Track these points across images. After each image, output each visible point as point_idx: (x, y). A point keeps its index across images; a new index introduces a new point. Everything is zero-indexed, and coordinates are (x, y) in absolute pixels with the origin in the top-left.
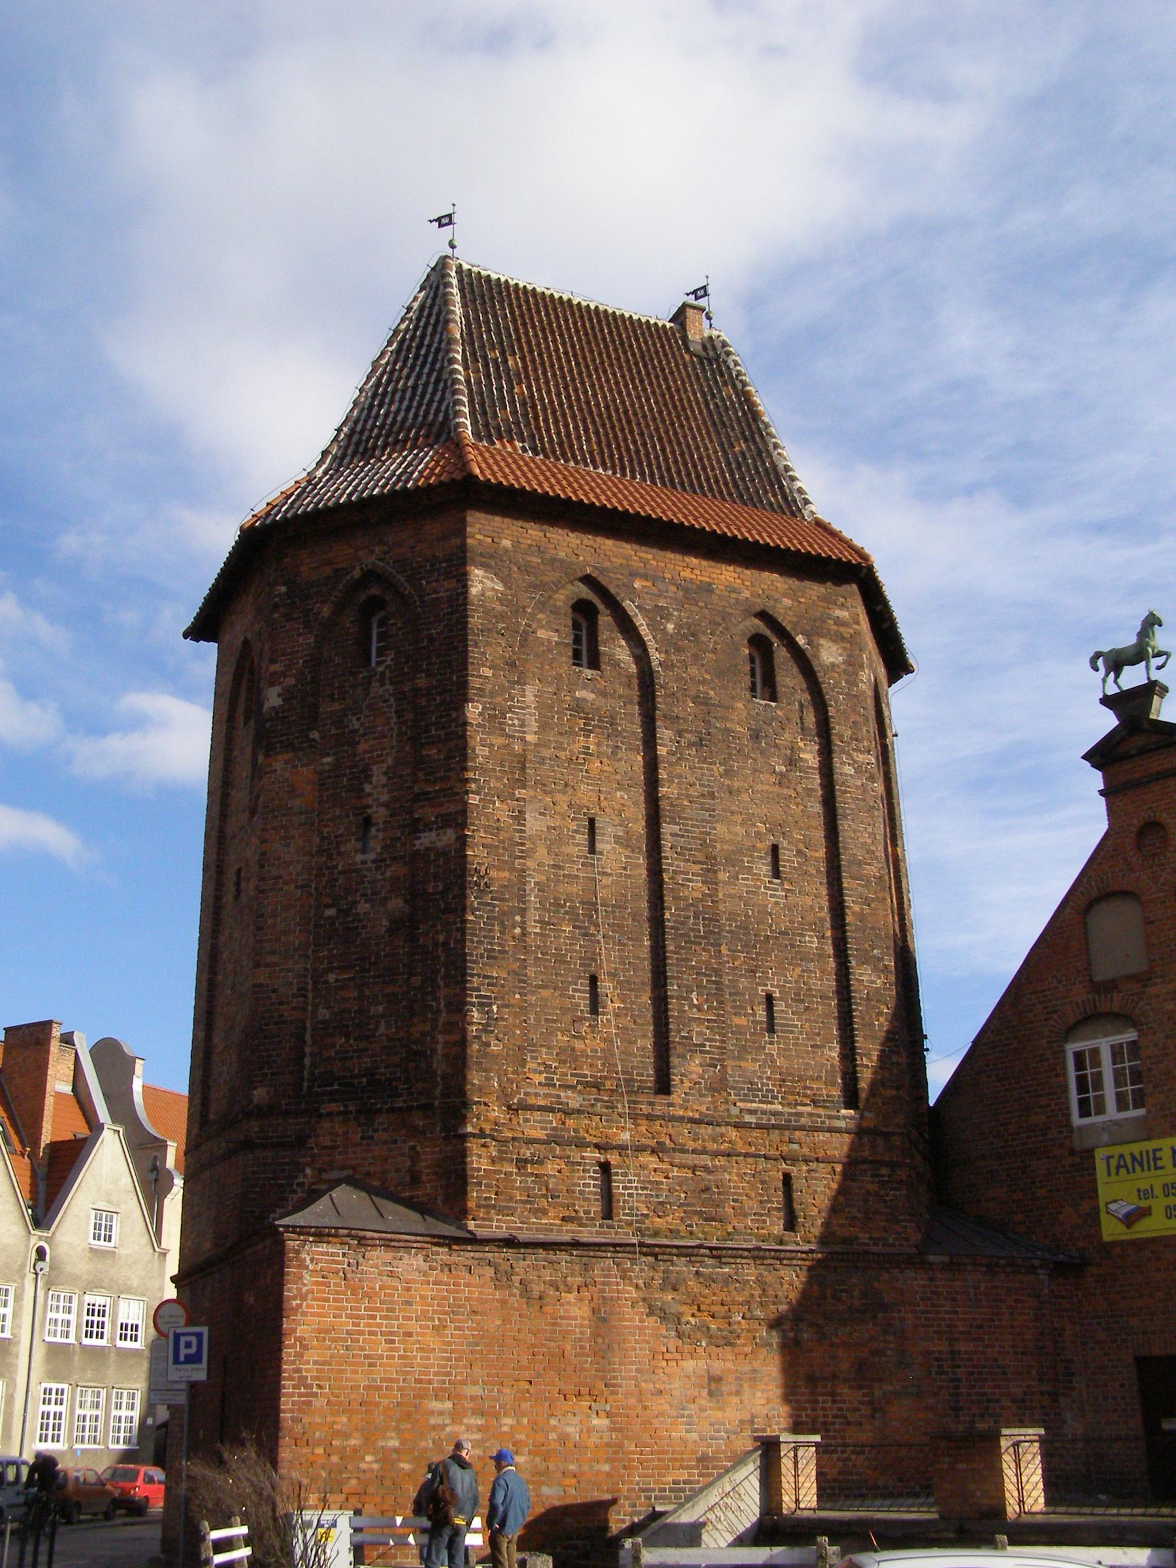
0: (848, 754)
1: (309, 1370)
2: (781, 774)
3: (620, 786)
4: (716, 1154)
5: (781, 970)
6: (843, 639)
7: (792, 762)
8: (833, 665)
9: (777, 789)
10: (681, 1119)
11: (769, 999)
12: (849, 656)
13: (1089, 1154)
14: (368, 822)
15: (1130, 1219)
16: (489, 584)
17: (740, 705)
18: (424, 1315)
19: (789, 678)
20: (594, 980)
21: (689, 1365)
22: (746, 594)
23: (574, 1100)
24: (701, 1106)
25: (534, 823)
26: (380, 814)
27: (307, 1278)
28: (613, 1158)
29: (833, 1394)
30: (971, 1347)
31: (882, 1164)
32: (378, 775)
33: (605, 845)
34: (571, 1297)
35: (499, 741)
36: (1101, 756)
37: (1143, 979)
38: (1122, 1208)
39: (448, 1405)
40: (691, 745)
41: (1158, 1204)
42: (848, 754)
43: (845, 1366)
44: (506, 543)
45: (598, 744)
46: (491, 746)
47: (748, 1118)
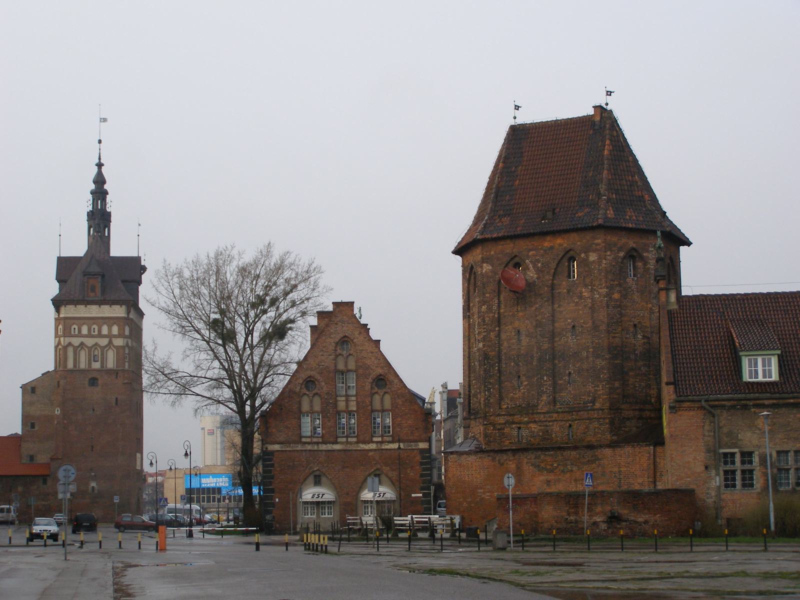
0: (597, 291)
2: (577, 302)
3: (527, 319)
4: (549, 422)
6: (598, 250)
7: (581, 297)
8: (594, 261)
9: (575, 307)
10: (540, 413)
11: (570, 373)
12: (600, 256)
16: (488, 268)
17: (564, 283)
18: (476, 470)
20: (519, 377)
21: (542, 478)
22: (565, 245)
24: (545, 410)
25: (503, 336)
27: (450, 463)
28: (522, 426)
29: (582, 484)
30: (625, 469)
31: (600, 418)
33: (523, 338)
34: (511, 463)
35: (492, 315)
39: (482, 491)
40: (546, 301)
42: (597, 291)
44: (492, 253)
45: (521, 308)
46: (489, 317)
47: (559, 410)
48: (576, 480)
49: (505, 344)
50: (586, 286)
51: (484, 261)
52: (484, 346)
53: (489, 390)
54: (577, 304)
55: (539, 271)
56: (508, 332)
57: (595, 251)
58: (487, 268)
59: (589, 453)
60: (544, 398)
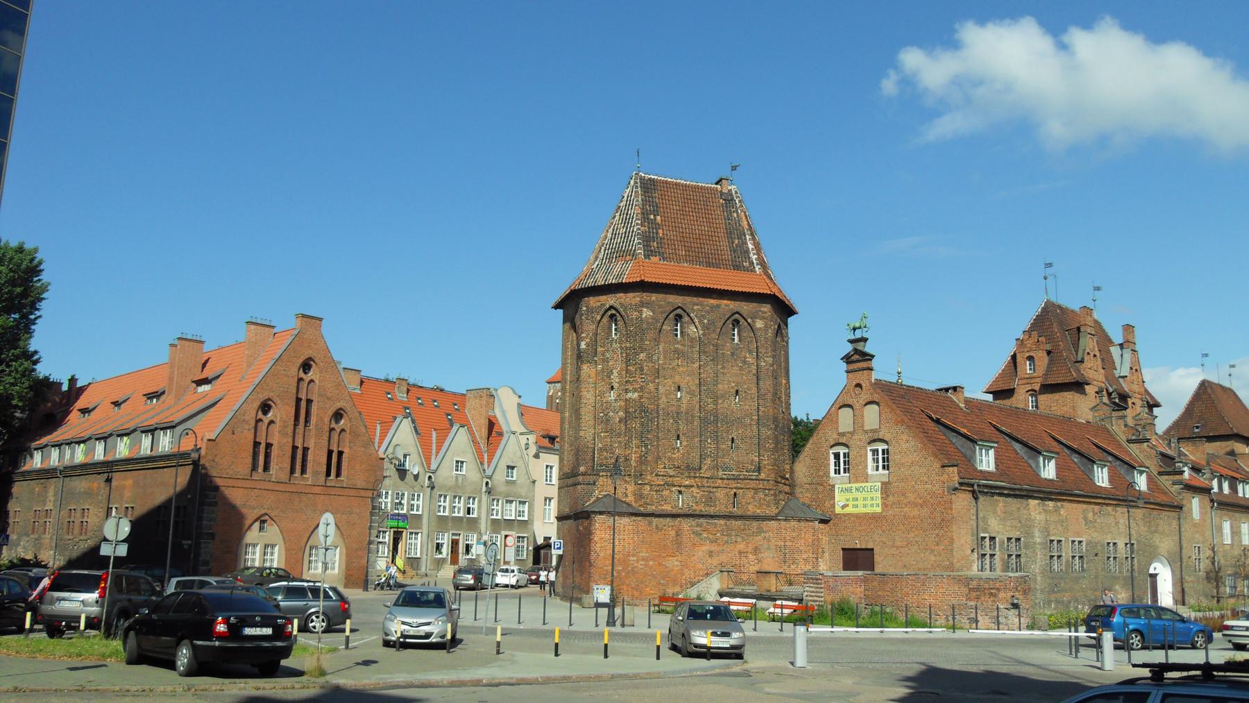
1: (598, 549)
5: (737, 429)
7: (745, 362)
13: (833, 486)
14: (612, 388)
15: (843, 507)
19: (747, 333)
21: (704, 548)
23: (671, 472)
25: (661, 389)
26: (616, 386)
28: (682, 489)
32: (615, 373)
36: (847, 359)
37: (852, 433)
38: (841, 504)
41: (851, 503)
43: (750, 550)
48: (740, 552)
49: (664, 399)
50: (750, 352)
51: (643, 304)
52: (641, 397)
53: (646, 446)
54: (741, 369)
55: (705, 328)
56: (666, 386)
57: (762, 318)
58: (646, 313)
59: (755, 524)
60: (708, 461)
